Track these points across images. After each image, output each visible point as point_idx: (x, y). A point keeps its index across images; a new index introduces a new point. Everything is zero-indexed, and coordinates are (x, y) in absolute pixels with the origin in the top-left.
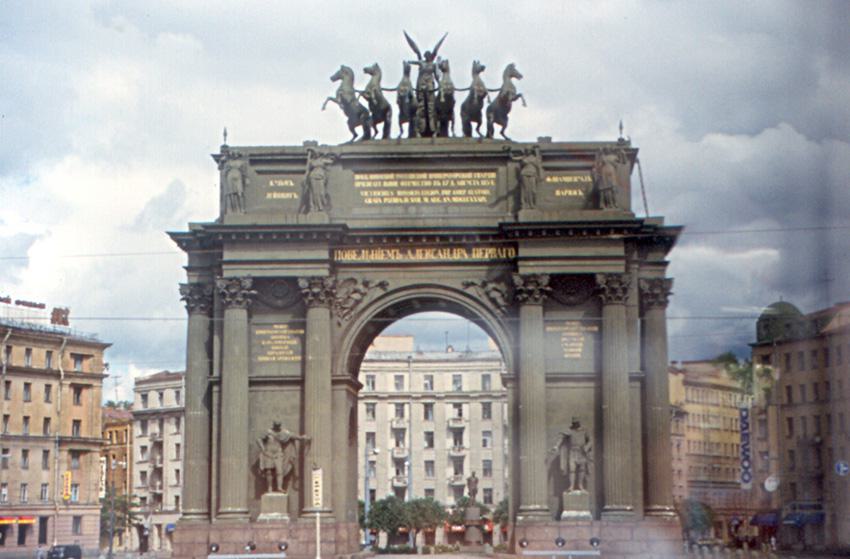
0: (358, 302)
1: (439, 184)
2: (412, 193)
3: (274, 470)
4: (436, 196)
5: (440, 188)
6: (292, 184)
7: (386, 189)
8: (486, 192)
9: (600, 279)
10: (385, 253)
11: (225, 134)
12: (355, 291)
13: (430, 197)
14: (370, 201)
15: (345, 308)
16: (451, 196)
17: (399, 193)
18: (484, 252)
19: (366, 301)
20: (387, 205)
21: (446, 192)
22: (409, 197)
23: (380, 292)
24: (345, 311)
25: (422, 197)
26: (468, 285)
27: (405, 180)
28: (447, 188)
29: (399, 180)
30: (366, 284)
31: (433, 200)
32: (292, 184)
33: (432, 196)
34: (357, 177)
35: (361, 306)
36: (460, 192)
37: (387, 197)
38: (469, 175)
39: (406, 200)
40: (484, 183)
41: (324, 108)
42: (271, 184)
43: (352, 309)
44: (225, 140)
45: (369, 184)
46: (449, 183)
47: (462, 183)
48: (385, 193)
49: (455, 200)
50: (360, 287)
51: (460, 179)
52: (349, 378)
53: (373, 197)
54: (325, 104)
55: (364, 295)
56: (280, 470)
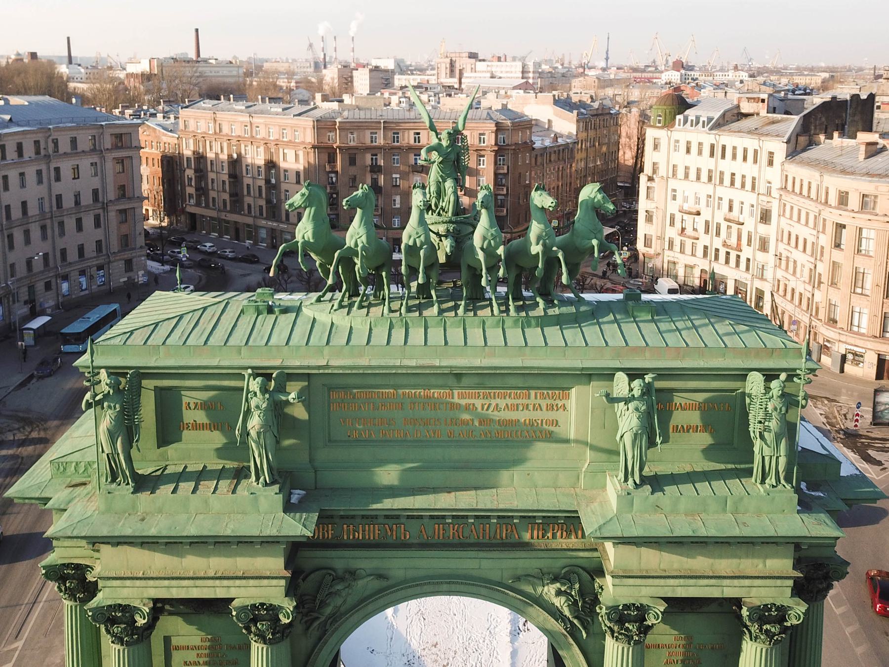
23: (377, 584)
30: (353, 574)
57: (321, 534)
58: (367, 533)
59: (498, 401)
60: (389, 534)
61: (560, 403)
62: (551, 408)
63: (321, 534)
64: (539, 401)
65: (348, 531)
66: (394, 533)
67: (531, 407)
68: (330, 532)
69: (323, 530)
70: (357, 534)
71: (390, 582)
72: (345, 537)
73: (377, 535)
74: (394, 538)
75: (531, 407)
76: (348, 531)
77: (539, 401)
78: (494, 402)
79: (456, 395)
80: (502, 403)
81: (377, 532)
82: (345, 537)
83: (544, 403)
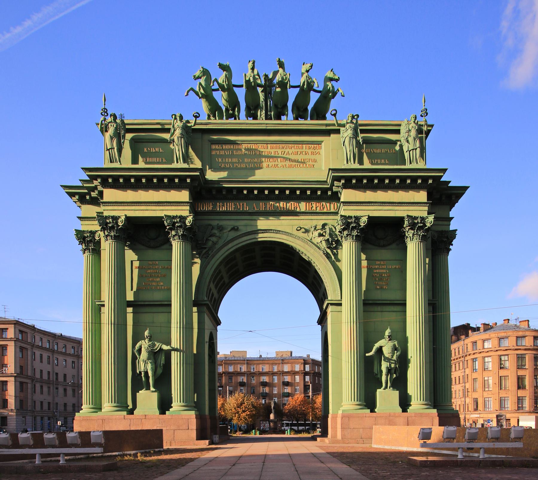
3: (146, 373)
6: (161, 151)
10: (235, 205)
12: (212, 235)
14: (223, 166)
15: (205, 248)
19: (221, 243)
20: (237, 169)
23: (233, 234)
24: (204, 251)
26: (299, 229)
30: (221, 228)
32: (161, 151)
34: (213, 147)
35: (218, 246)
37: (236, 163)
41: (187, 95)
42: (145, 150)
43: (209, 249)
45: (222, 153)
48: (234, 160)
52: (208, 302)
53: (225, 163)
54: (188, 92)
55: (220, 237)
56: (150, 374)
57: (207, 208)
58: (228, 207)
59: (288, 150)
60: (239, 207)
61: (317, 151)
62: (312, 153)
63: (207, 208)
64: (307, 150)
65: (220, 206)
66: (241, 207)
67: (304, 153)
68: (211, 207)
69: (208, 205)
70: (223, 207)
71: (239, 233)
72: (218, 210)
73: (233, 208)
74: (241, 210)
75: (304, 153)
76: (220, 206)
77: (307, 150)
78: (286, 151)
79: (269, 147)
80: (290, 151)
81: (233, 206)
82: (218, 210)
83: (310, 151)
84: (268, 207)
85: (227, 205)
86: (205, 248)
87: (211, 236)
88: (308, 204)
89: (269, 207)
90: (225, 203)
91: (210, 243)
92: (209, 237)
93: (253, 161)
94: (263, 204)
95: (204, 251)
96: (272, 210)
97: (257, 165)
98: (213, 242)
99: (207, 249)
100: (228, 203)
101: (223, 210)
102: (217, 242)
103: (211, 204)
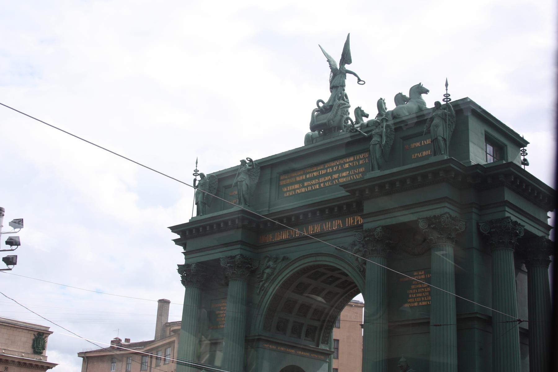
0: (269, 275)
1: (331, 171)
2: (314, 182)
4: (328, 181)
5: (331, 174)
7: (298, 182)
8: (361, 170)
9: (422, 225)
11: (197, 163)
13: (324, 182)
15: (263, 281)
16: (339, 178)
17: (306, 184)
18: (354, 219)
20: (298, 194)
21: (336, 176)
22: (311, 185)
24: (261, 284)
25: (319, 184)
27: (309, 173)
28: (335, 173)
29: (306, 174)
31: (327, 184)
33: (326, 181)
36: (344, 174)
37: (298, 189)
38: (352, 159)
39: (310, 188)
40: (361, 162)
44: (196, 166)
46: (338, 167)
47: (347, 166)
48: (297, 186)
49: (341, 180)
50: (271, 263)
51: (345, 163)
53: (290, 191)
55: (274, 269)
70: (280, 237)
72: (276, 240)
84: (315, 230)
85: (283, 234)
86: (263, 281)
87: (268, 267)
88: (350, 218)
89: (316, 229)
90: (282, 232)
91: (265, 276)
92: (265, 269)
93: (311, 183)
94: (312, 226)
95: (261, 284)
96: (319, 232)
97: (314, 187)
98: (268, 274)
99: (264, 282)
100: (284, 232)
101: (280, 239)
102: (273, 273)
103: (271, 235)
